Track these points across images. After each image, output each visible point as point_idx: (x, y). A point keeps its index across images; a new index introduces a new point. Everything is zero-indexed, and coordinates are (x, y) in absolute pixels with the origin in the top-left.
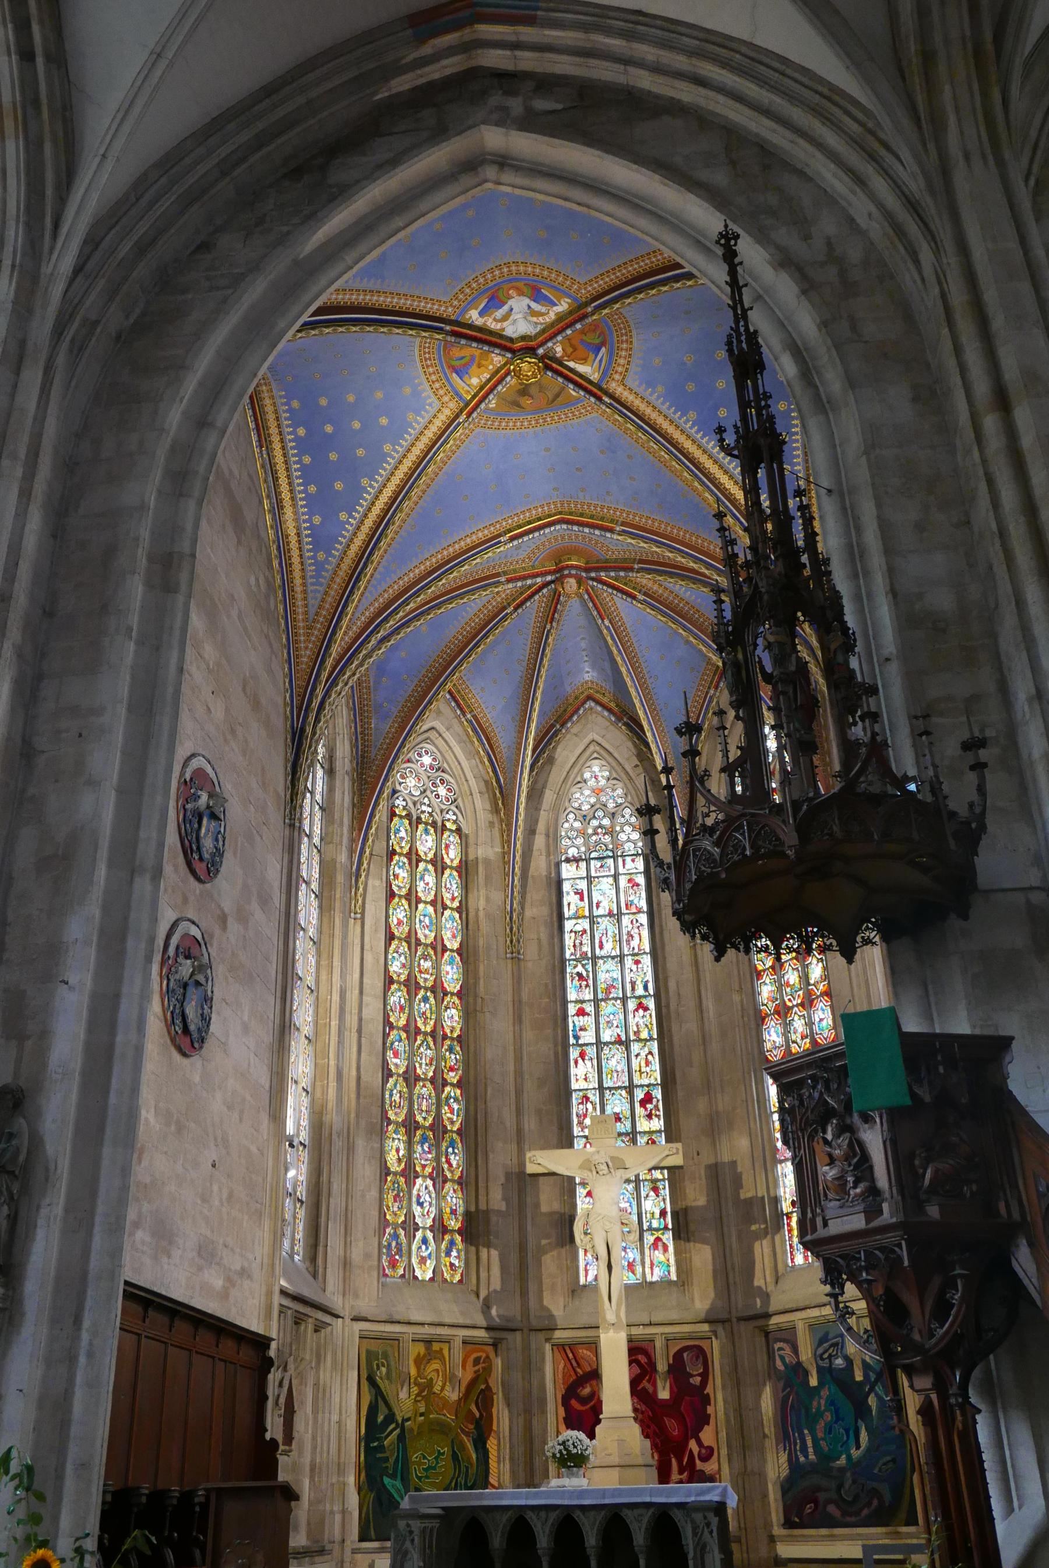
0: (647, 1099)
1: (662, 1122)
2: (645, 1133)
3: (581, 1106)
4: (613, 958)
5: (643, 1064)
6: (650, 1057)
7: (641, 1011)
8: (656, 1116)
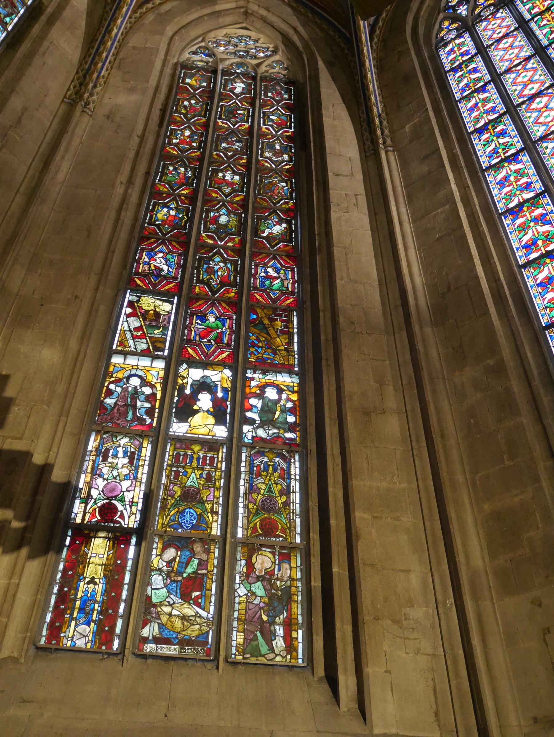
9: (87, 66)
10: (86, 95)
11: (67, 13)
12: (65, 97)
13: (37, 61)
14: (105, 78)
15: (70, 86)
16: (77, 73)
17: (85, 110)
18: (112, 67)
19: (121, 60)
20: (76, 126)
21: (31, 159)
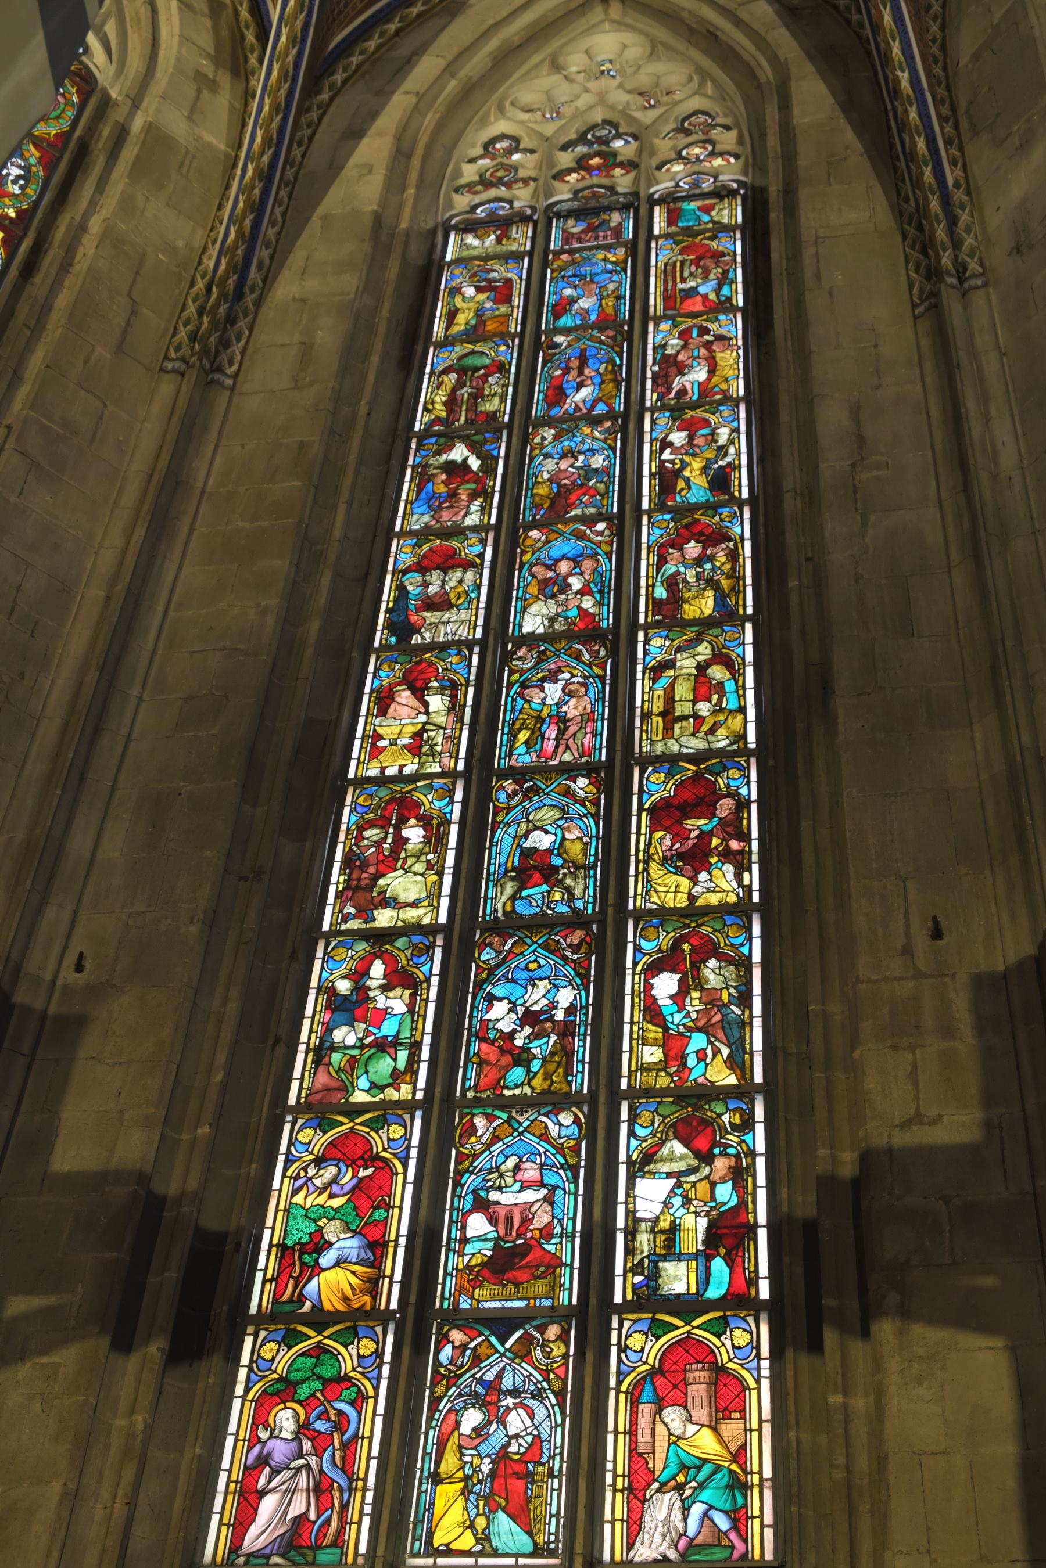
0: (696, 797)
1: (754, 877)
2: (664, 914)
3: (372, 834)
4: (595, 421)
5: (683, 691)
6: (717, 672)
7: (693, 549)
8: (727, 855)
9: (912, 203)
10: (946, 260)
11: (806, 156)
12: (914, 306)
13: (815, 303)
14: (962, 181)
15: (908, 275)
16: (904, 237)
17: (966, 285)
18: (961, 149)
19: (968, 111)
20: (971, 336)
21: (934, 484)
